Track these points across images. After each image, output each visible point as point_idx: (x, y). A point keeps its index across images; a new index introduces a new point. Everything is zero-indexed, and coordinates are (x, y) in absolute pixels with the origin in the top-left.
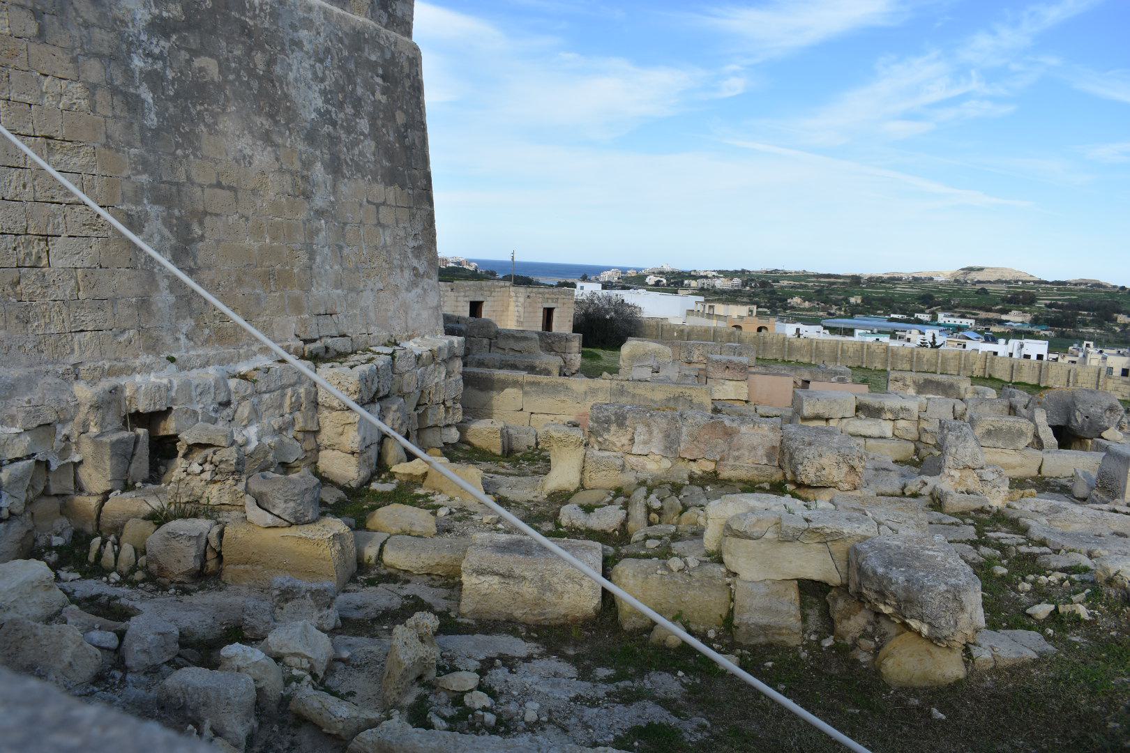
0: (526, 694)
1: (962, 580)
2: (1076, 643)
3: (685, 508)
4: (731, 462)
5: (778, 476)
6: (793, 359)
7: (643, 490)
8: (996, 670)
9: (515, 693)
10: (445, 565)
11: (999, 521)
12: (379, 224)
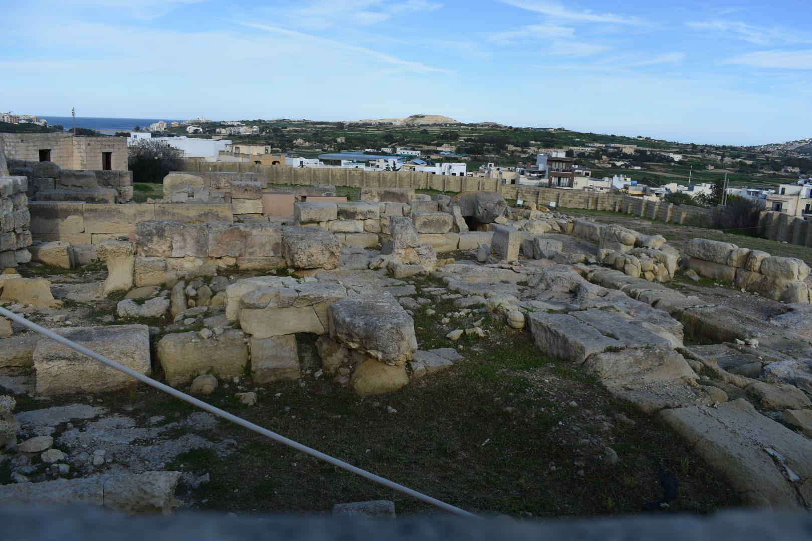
0: (94, 445)
1: (401, 320)
2: (476, 352)
3: (214, 293)
4: (247, 257)
5: (282, 264)
6: (298, 183)
7: (182, 283)
8: (428, 376)
9: (85, 446)
10: (22, 358)
11: (430, 280)
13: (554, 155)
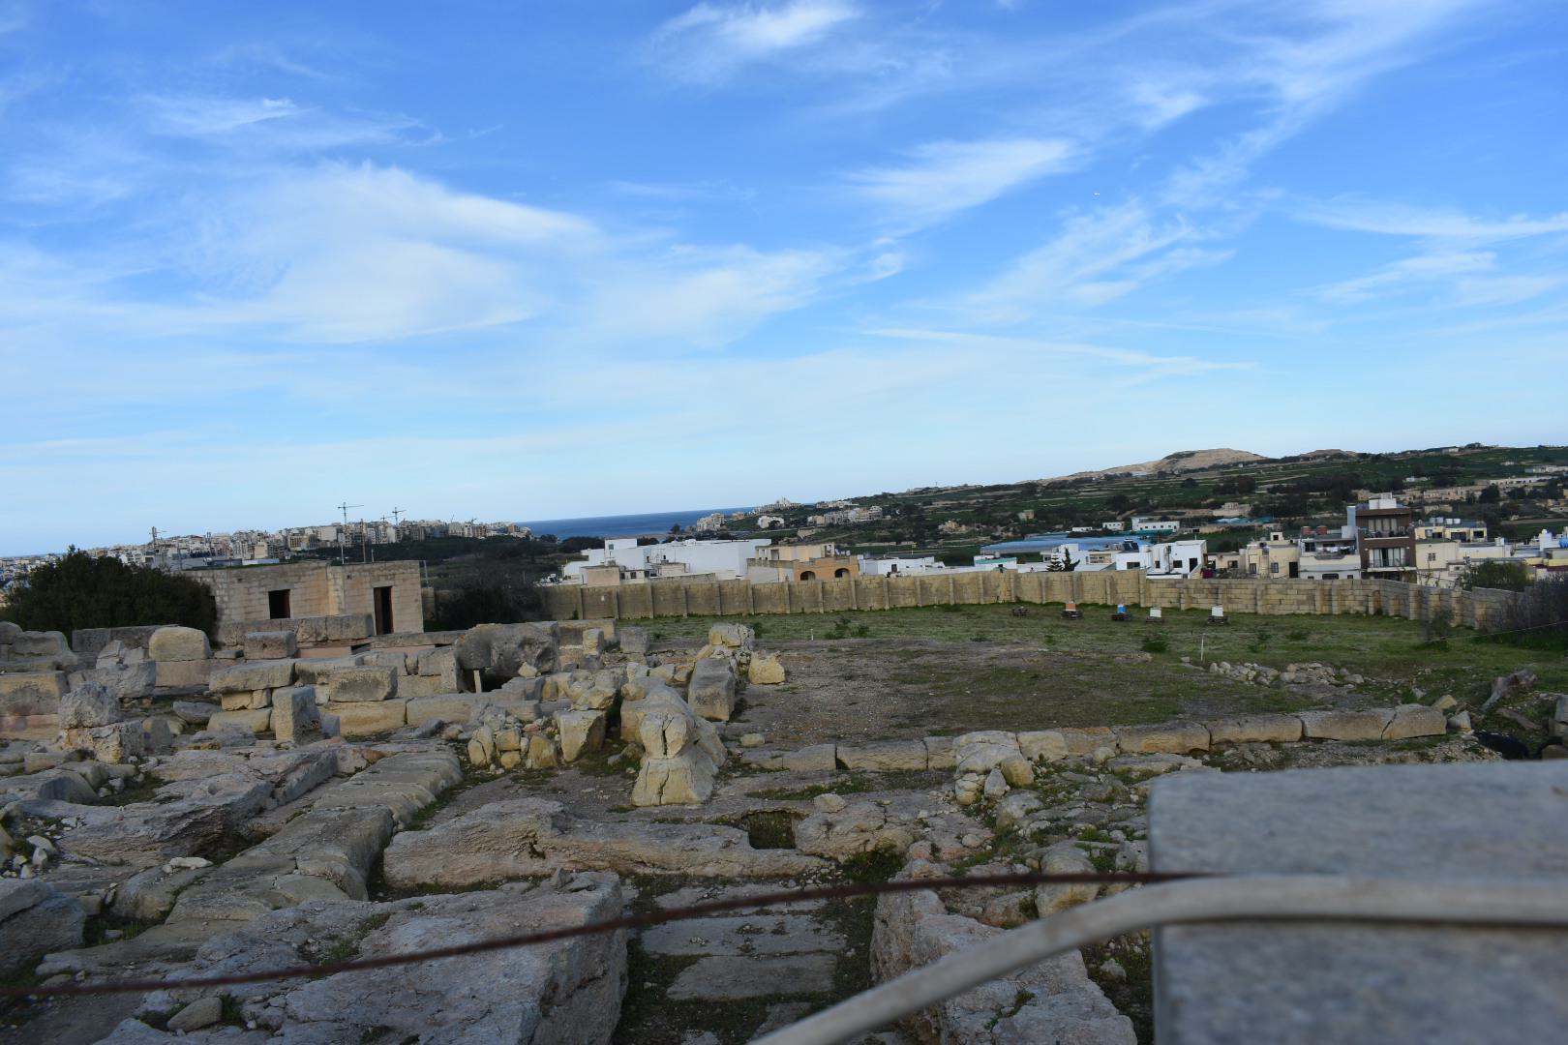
6: (764, 610)
13: (1373, 505)
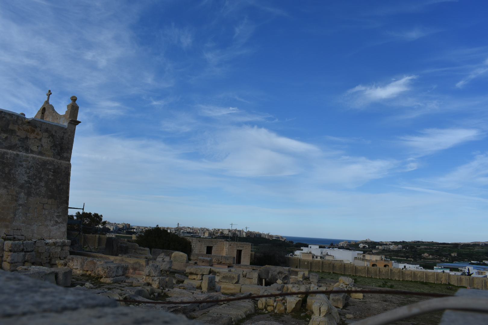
6: (358, 275)
12: (43, 208)
